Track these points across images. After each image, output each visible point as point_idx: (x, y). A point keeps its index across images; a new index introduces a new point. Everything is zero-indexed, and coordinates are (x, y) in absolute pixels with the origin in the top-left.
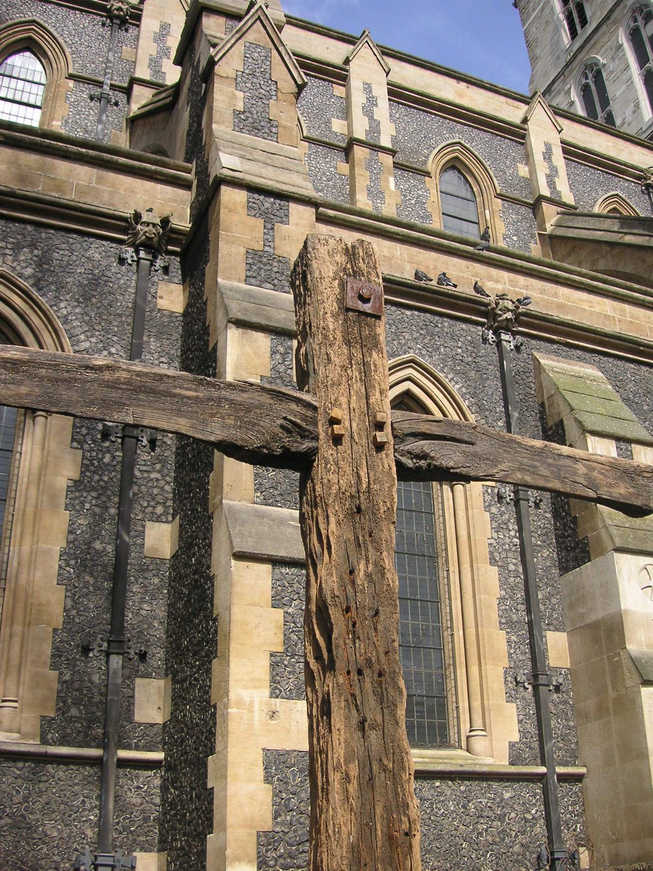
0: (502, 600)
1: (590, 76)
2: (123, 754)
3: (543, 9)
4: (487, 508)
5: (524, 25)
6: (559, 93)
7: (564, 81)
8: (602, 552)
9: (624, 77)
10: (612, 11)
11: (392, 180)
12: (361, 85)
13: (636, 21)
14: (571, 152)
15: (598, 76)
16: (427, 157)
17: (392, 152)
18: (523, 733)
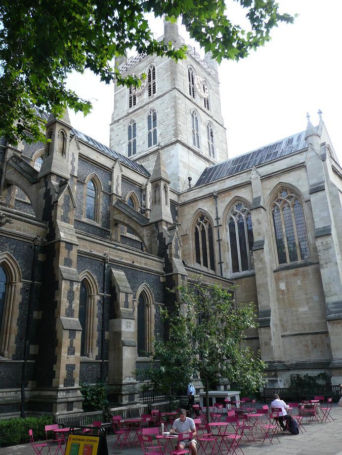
0: (98, 325)
1: (132, 124)
2: (28, 361)
3: (122, 91)
4: (98, 305)
5: (115, 92)
6: (120, 124)
7: (123, 121)
8: (119, 318)
9: (143, 131)
10: (144, 106)
11: (76, 186)
12: (71, 154)
13: (151, 113)
14: (124, 178)
15: (135, 124)
16: (86, 177)
17: (77, 177)
18: (99, 353)
